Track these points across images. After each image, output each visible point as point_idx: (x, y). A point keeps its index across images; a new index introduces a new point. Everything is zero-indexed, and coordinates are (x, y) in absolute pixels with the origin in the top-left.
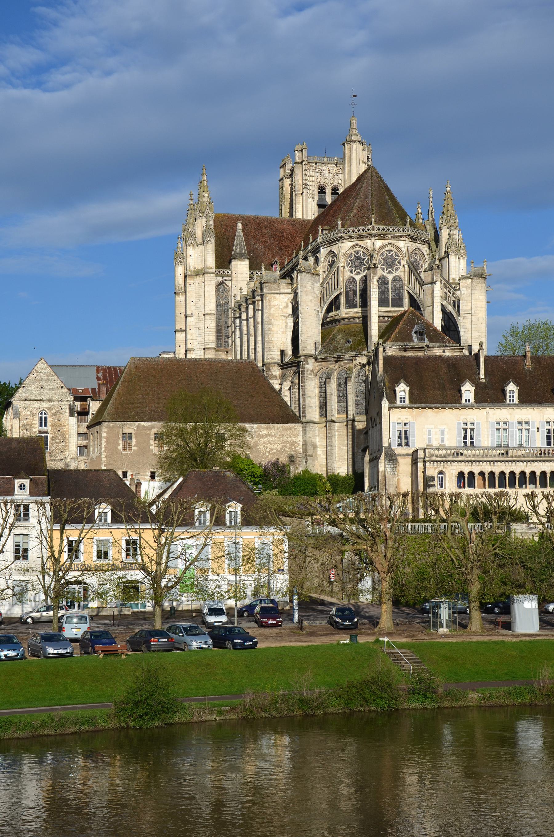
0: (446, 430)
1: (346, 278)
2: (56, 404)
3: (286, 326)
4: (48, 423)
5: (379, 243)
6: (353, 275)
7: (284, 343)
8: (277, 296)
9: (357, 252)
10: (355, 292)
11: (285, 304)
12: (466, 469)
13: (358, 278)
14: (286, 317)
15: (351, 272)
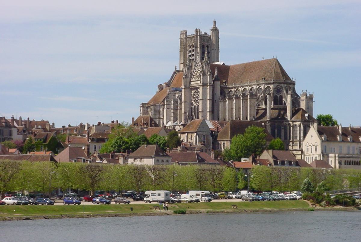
0: (335, 149)
1: (275, 95)
2: (207, 133)
3: (255, 109)
4: (205, 139)
5: (285, 85)
6: (277, 95)
7: (254, 114)
8: (253, 99)
9: (278, 88)
10: (277, 100)
11: (254, 102)
12: (347, 159)
13: (278, 96)
14: (255, 106)
15: (276, 93)
